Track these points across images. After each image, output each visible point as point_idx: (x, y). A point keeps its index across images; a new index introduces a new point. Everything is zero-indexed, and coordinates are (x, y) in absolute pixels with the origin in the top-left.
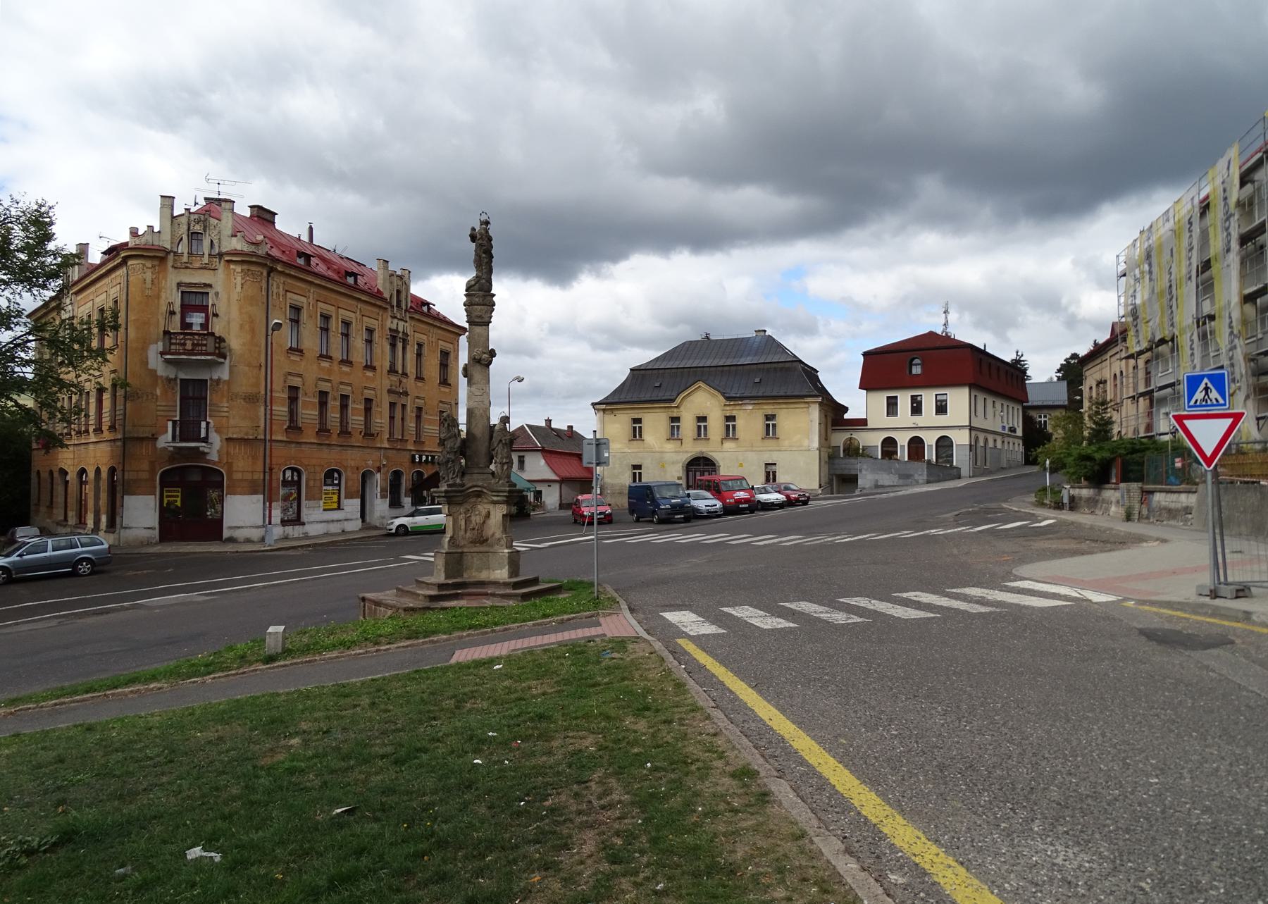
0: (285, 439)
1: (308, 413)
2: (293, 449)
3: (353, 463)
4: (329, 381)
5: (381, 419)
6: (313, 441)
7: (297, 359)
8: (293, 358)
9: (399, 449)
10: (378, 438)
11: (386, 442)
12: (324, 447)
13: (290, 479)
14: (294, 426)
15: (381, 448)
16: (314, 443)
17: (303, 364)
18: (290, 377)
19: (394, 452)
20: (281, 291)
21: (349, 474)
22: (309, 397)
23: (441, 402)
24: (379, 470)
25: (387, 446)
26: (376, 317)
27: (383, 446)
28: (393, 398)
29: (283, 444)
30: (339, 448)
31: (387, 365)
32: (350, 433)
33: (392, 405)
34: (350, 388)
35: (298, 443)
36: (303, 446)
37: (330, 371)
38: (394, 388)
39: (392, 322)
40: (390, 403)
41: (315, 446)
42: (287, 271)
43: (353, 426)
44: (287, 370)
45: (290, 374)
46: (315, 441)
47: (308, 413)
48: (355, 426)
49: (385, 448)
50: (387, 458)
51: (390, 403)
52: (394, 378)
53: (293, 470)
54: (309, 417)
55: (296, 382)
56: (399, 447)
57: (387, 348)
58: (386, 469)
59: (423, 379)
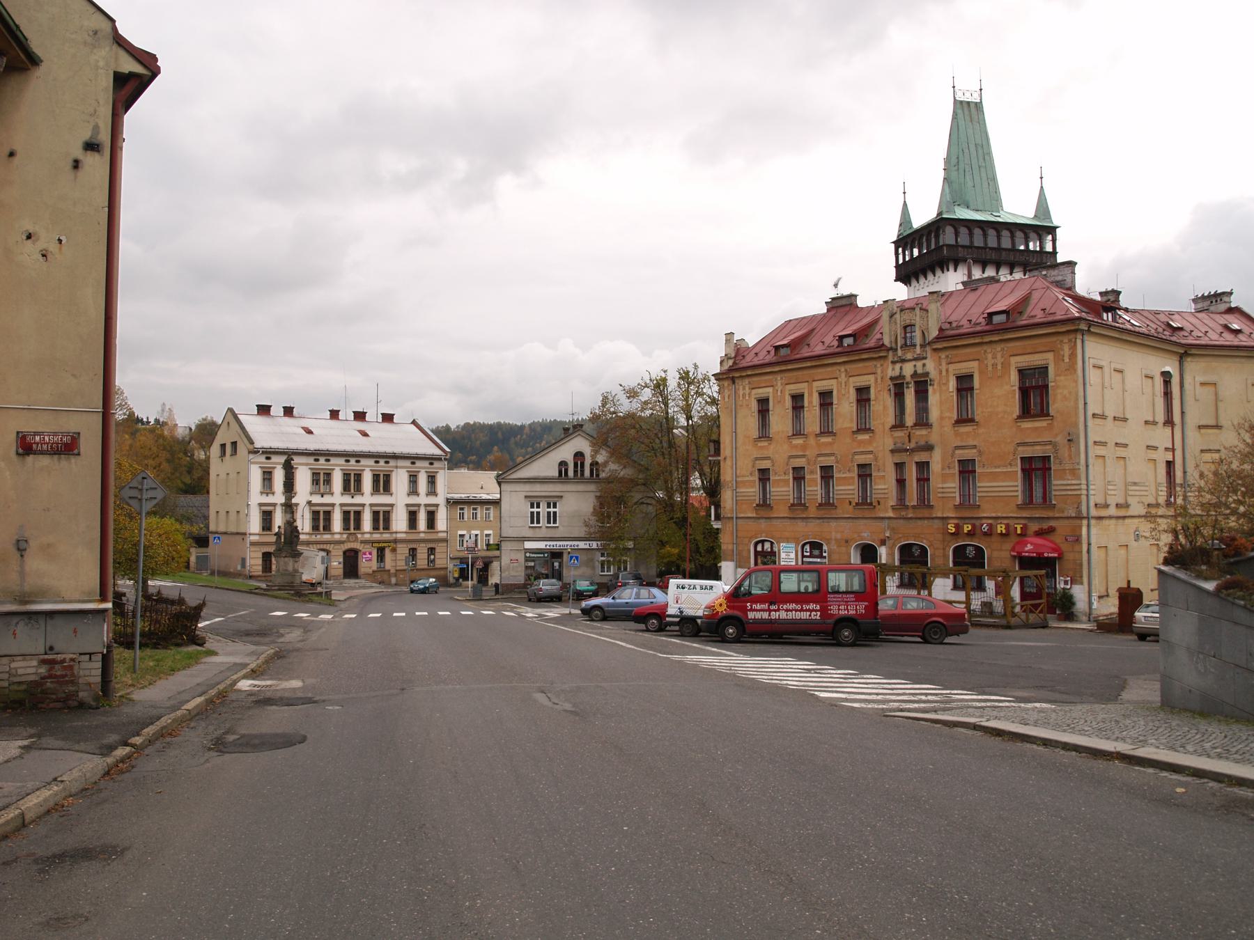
0: (754, 515)
1: (782, 490)
2: (763, 524)
3: (839, 536)
4: (803, 456)
5: (885, 485)
6: (750, 515)
7: (766, 444)
8: (759, 445)
9: (911, 518)
10: (881, 506)
11: (890, 510)
12: (799, 521)
13: (769, 550)
14: (764, 505)
15: (883, 518)
16: (787, 517)
17: (772, 447)
18: (757, 462)
19: (902, 521)
20: (747, 391)
21: (834, 547)
22: (779, 475)
23: (1019, 444)
24: (883, 543)
25: (891, 514)
26: (874, 371)
27: (887, 515)
28: (898, 458)
29: (753, 520)
30: (818, 521)
31: (891, 420)
32: (833, 505)
33: (899, 466)
34: (833, 458)
35: (766, 518)
36: (775, 520)
37: (804, 447)
38: (899, 445)
39: (893, 369)
40: (896, 464)
41: (788, 520)
42: (744, 374)
43: (838, 497)
44: (755, 456)
45: (757, 459)
46: (789, 516)
47: (782, 490)
48: (841, 497)
49: (890, 518)
50: (893, 530)
51: (896, 464)
52: (899, 434)
53: (763, 542)
54: (779, 493)
55: (765, 464)
56: (910, 516)
57: (889, 402)
58: (891, 542)
59: (972, 420)
